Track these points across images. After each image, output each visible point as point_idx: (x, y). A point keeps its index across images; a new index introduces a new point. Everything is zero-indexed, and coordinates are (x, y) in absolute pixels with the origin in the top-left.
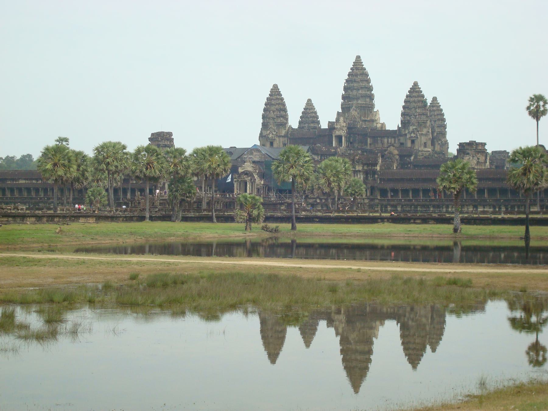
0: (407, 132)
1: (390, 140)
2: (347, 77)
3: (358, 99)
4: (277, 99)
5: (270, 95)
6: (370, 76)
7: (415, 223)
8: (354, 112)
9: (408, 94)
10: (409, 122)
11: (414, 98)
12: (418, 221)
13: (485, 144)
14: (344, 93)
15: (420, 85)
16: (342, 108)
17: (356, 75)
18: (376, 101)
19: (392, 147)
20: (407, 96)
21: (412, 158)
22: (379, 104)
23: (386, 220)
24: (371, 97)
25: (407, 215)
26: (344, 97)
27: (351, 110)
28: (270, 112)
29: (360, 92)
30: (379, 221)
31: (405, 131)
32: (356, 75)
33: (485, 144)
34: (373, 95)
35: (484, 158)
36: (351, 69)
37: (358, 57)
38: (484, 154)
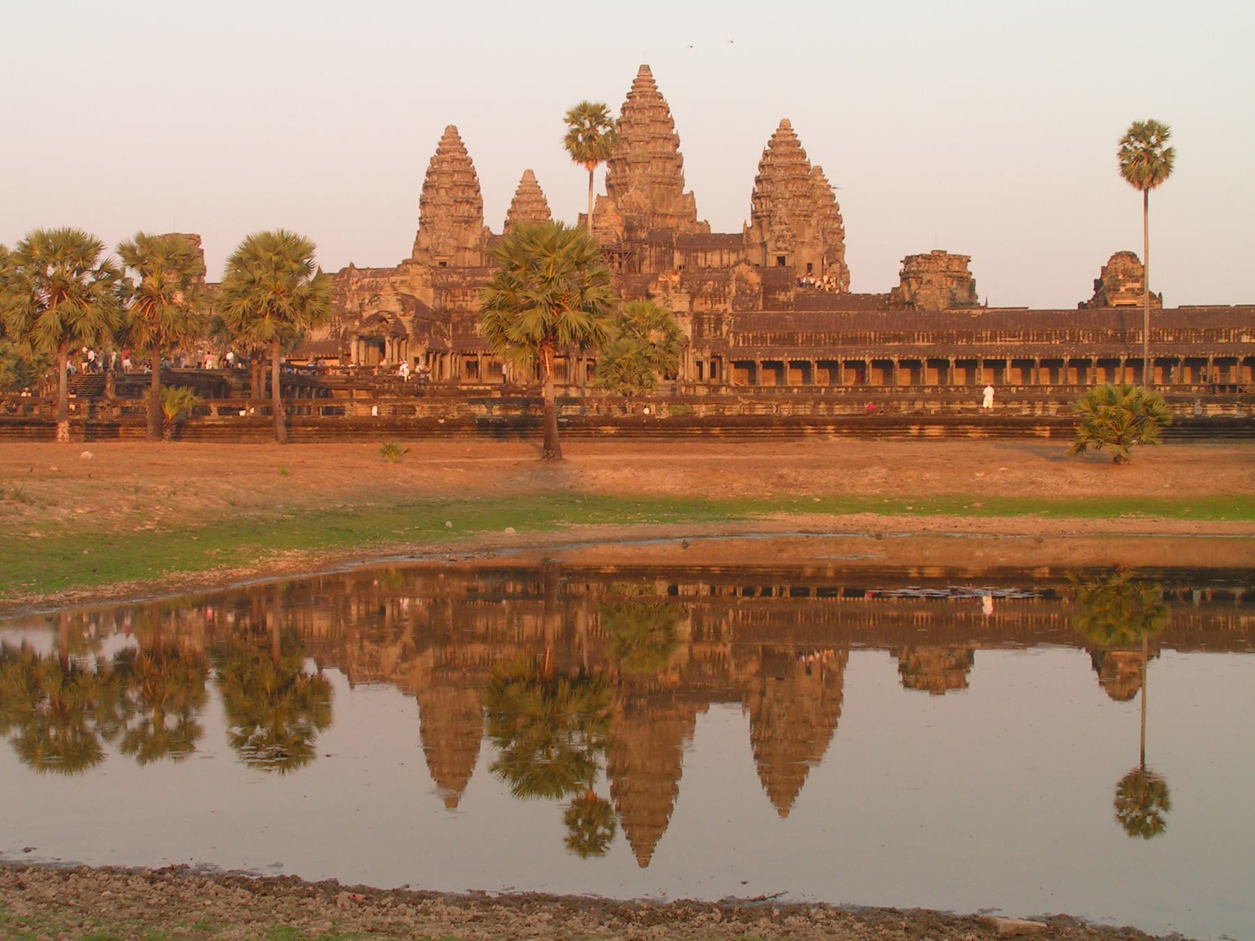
1: (725, 257)
4: (454, 159)
5: (438, 152)
6: (674, 113)
7: (921, 437)
8: (635, 195)
9: (768, 148)
12: (934, 431)
15: (797, 128)
20: (766, 154)
21: (792, 294)
22: (693, 179)
24: (676, 160)
25: (896, 409)
27: (631, 190)
29: (650, 147)
30: (809, 430)
32: (641, 109)
34: (680, 157)
35: (966, 294)
37: (645, 69)
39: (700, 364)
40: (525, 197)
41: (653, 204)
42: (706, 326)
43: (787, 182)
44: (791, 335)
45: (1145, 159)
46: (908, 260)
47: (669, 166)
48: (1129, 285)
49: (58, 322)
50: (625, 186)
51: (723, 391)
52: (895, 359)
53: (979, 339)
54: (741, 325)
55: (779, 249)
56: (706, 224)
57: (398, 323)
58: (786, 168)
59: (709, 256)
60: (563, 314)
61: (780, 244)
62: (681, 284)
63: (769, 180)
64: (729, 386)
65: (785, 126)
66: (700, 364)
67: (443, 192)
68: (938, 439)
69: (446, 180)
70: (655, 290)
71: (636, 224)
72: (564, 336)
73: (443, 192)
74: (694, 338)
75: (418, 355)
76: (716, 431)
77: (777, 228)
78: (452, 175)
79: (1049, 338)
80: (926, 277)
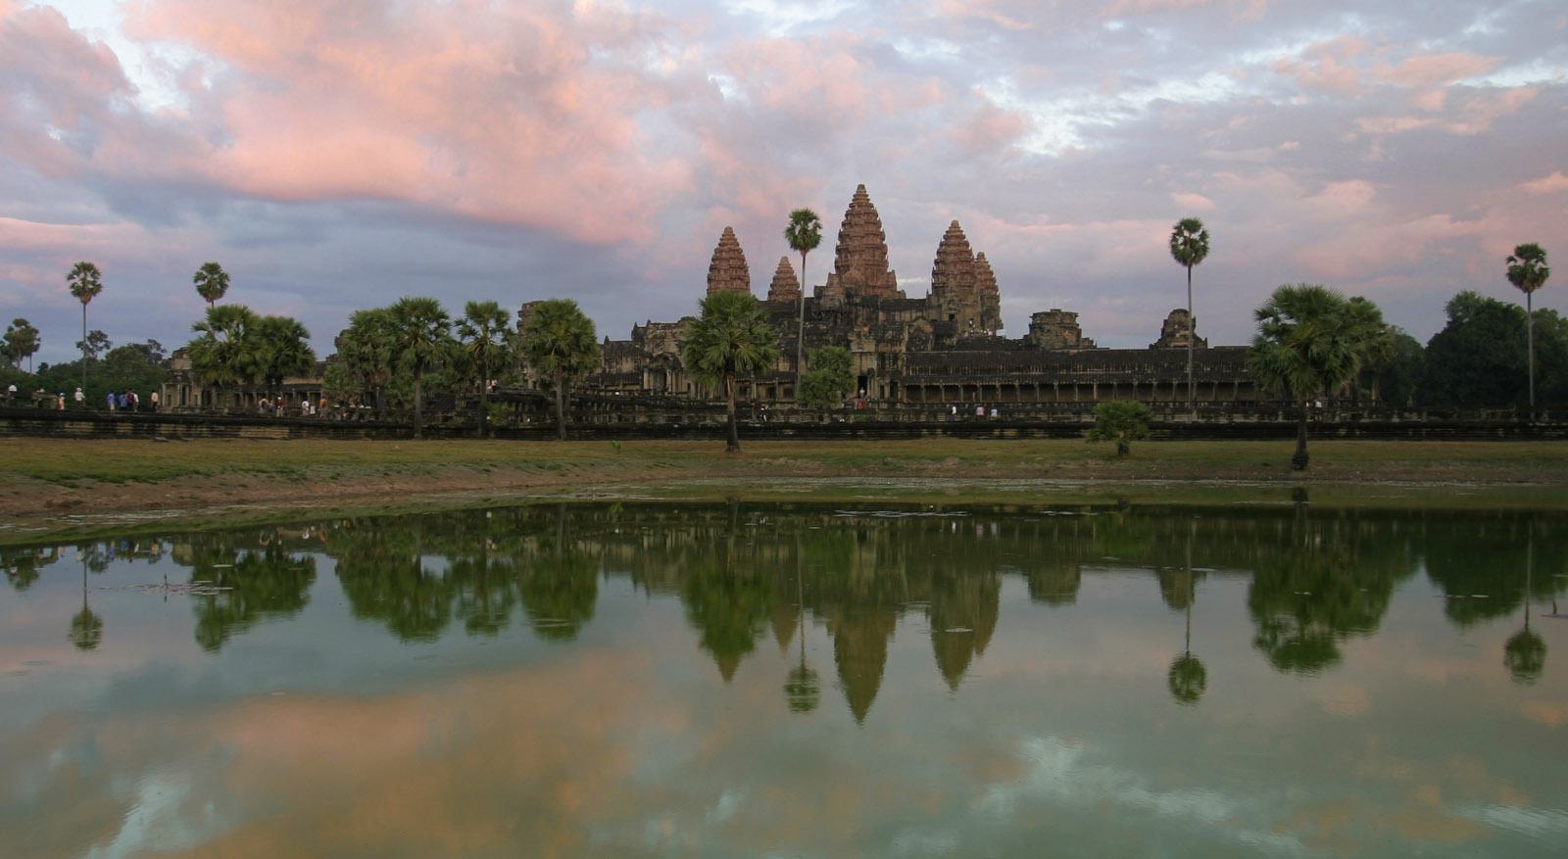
0: (942, 301)
2: (843, 218)
3: (861, 252)
4: (730, 250)
6: (881, 217)
7: (1001, 437)
8: (854, 273)
10: (944, 286)
11: (954, 246)
12: (1011, 432)
13: (1076, 315)
14: (839, 243)
16: (837, 267)
17: (859, 215)
18: (891, 256)
19: (921, 320)
20: (941, 244)
21: (955, 340)
22: (895, 259)
23: (939, 431)
24: (883, 249)
26: (838, 250)
28: (719, 272)
29: (865, 241)
30: (925, 432)
31: (938, 300)
32: (859, 215)
33: (1076, 315)
34: (885, 246)
35: (1075, 339)
36: (851, 206)
37: (861, 187)
38: (1075, 333)
39: (882, 388)
40: (782, 275)
41: (867, 278)
42: (887, 362)
43: (955, 263)
44: (945, 368)
45: (1189, 245)
46: (1035, 316)
47: (877, 253)
48: (1182, 332)
49: (414, 356)
50: (847, 268)
51: (899, 406)
52: (1017, 384)
53: (1074, 370)
54: (912, 360)
55: (950, 309)
56: (903, 293)
57: (676, 361)
58: (955, 254)
59: (903, 314)
60: (738, 350)
61: (951, 306)
62: (870, 333)
63: (943, 262)
64: (902, 403)
65: (955, 225)
66: (882, 388)
67: (722, 272)
68: (1014, 438)
69: (724, 264)
70: (852, 337)
71: (853, 293)
72: (738, 366)
73: (722, 272)
74: (878, 369)
75: (690, 382)
76: (861, 433)
77: (949, 295)
78: (729, 261)
79: (1124, 369)
80: (1047, 327)
